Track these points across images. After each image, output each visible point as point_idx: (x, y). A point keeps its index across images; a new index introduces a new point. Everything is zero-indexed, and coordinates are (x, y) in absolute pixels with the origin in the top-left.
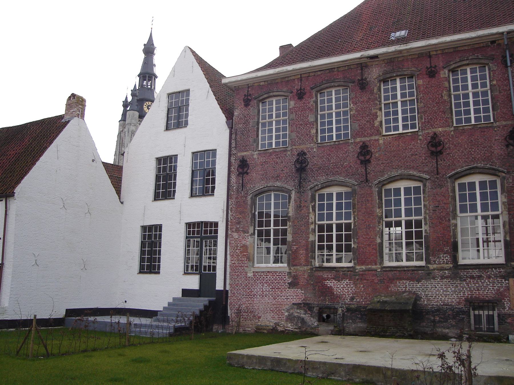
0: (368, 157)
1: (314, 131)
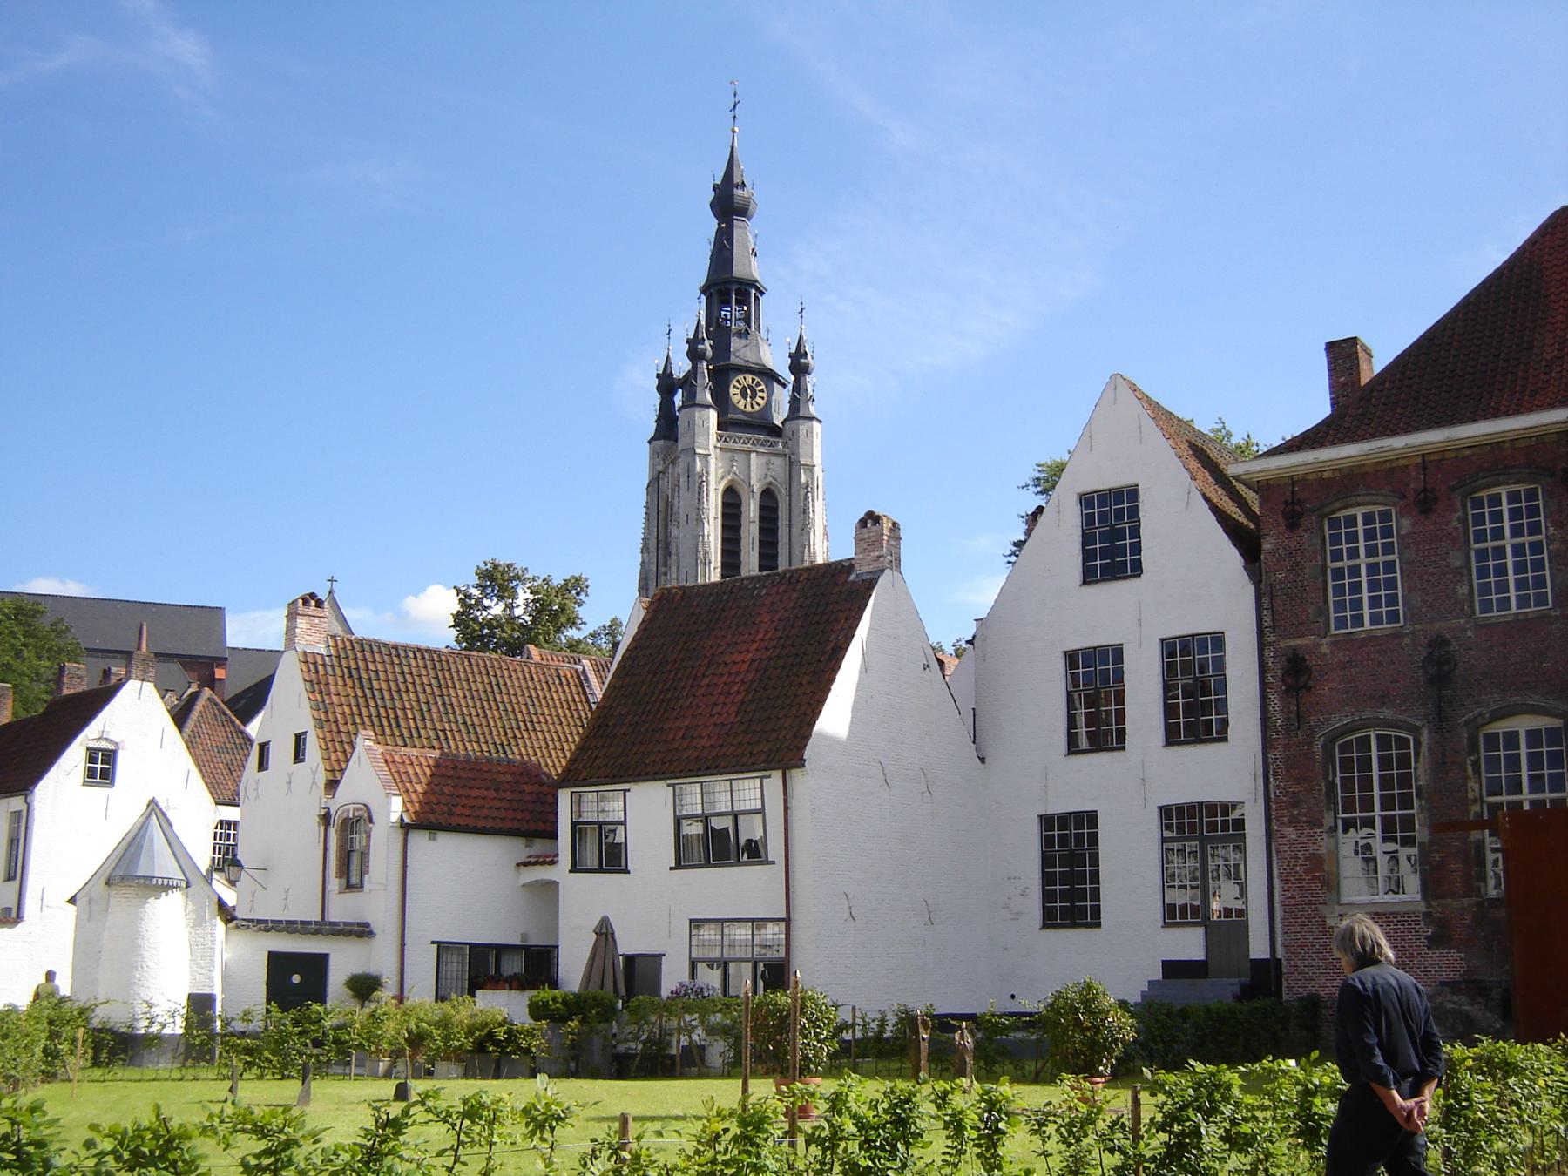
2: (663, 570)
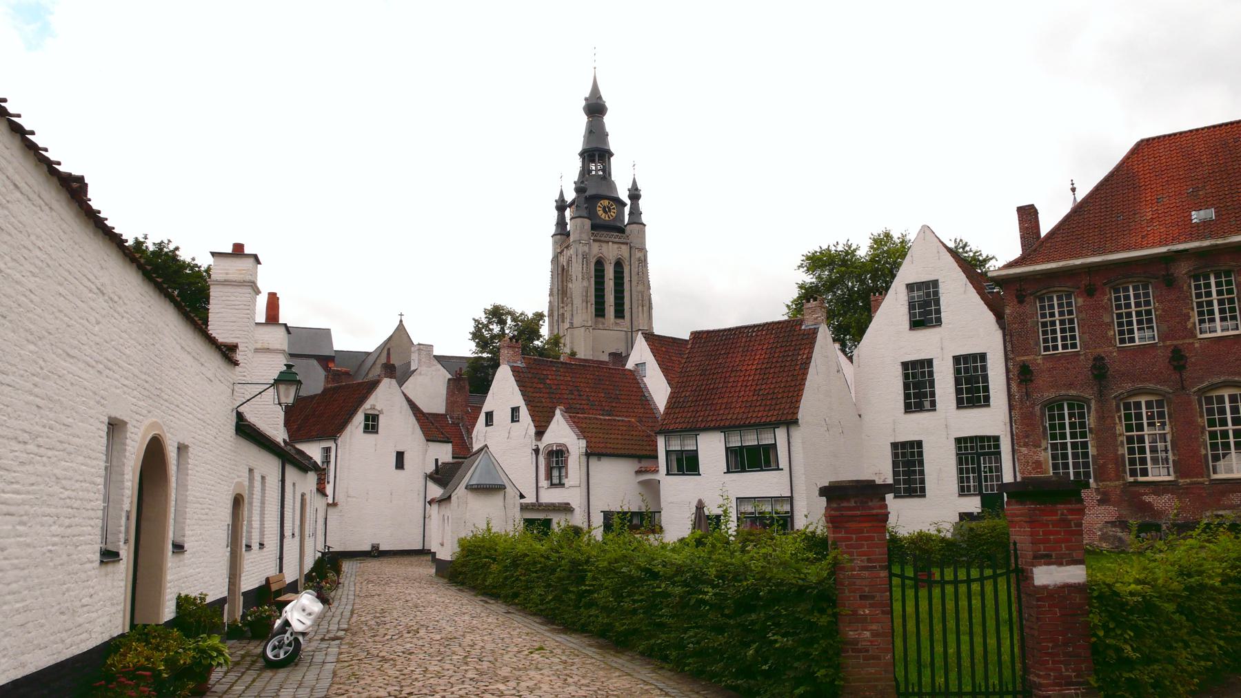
0: (1182, 363)
1: (1112, 333)
2: (562, 305)
